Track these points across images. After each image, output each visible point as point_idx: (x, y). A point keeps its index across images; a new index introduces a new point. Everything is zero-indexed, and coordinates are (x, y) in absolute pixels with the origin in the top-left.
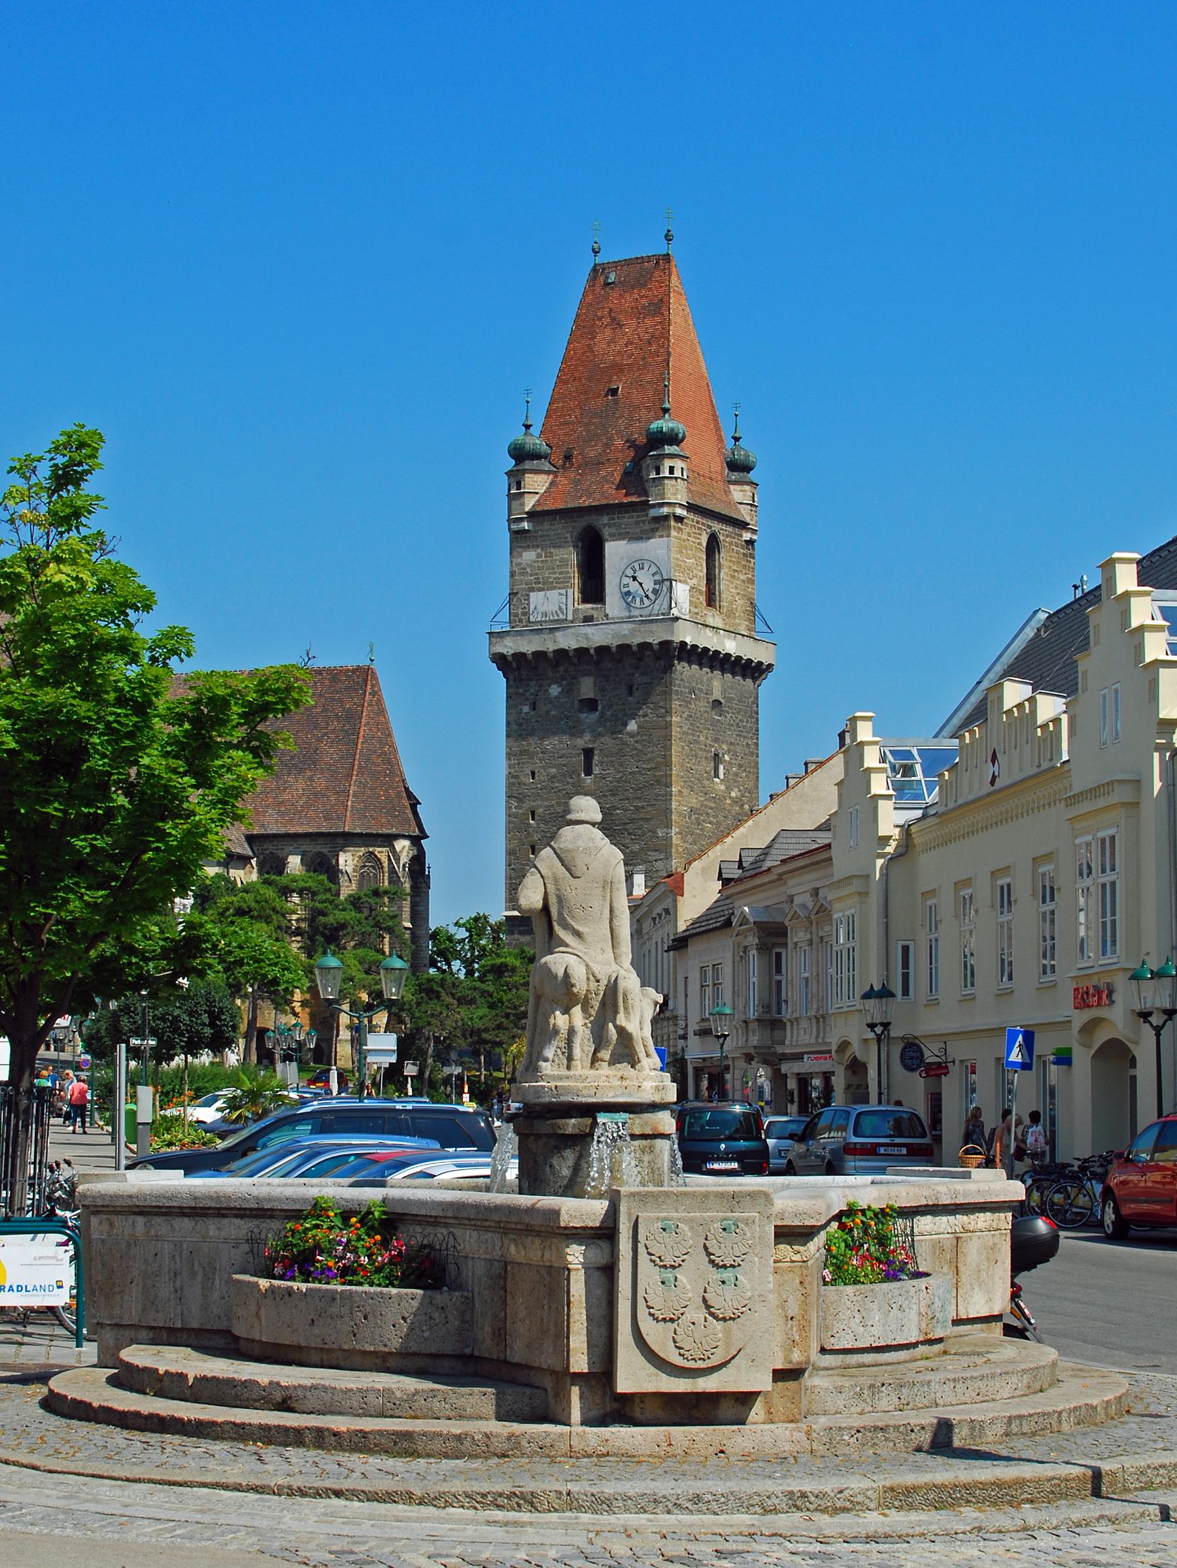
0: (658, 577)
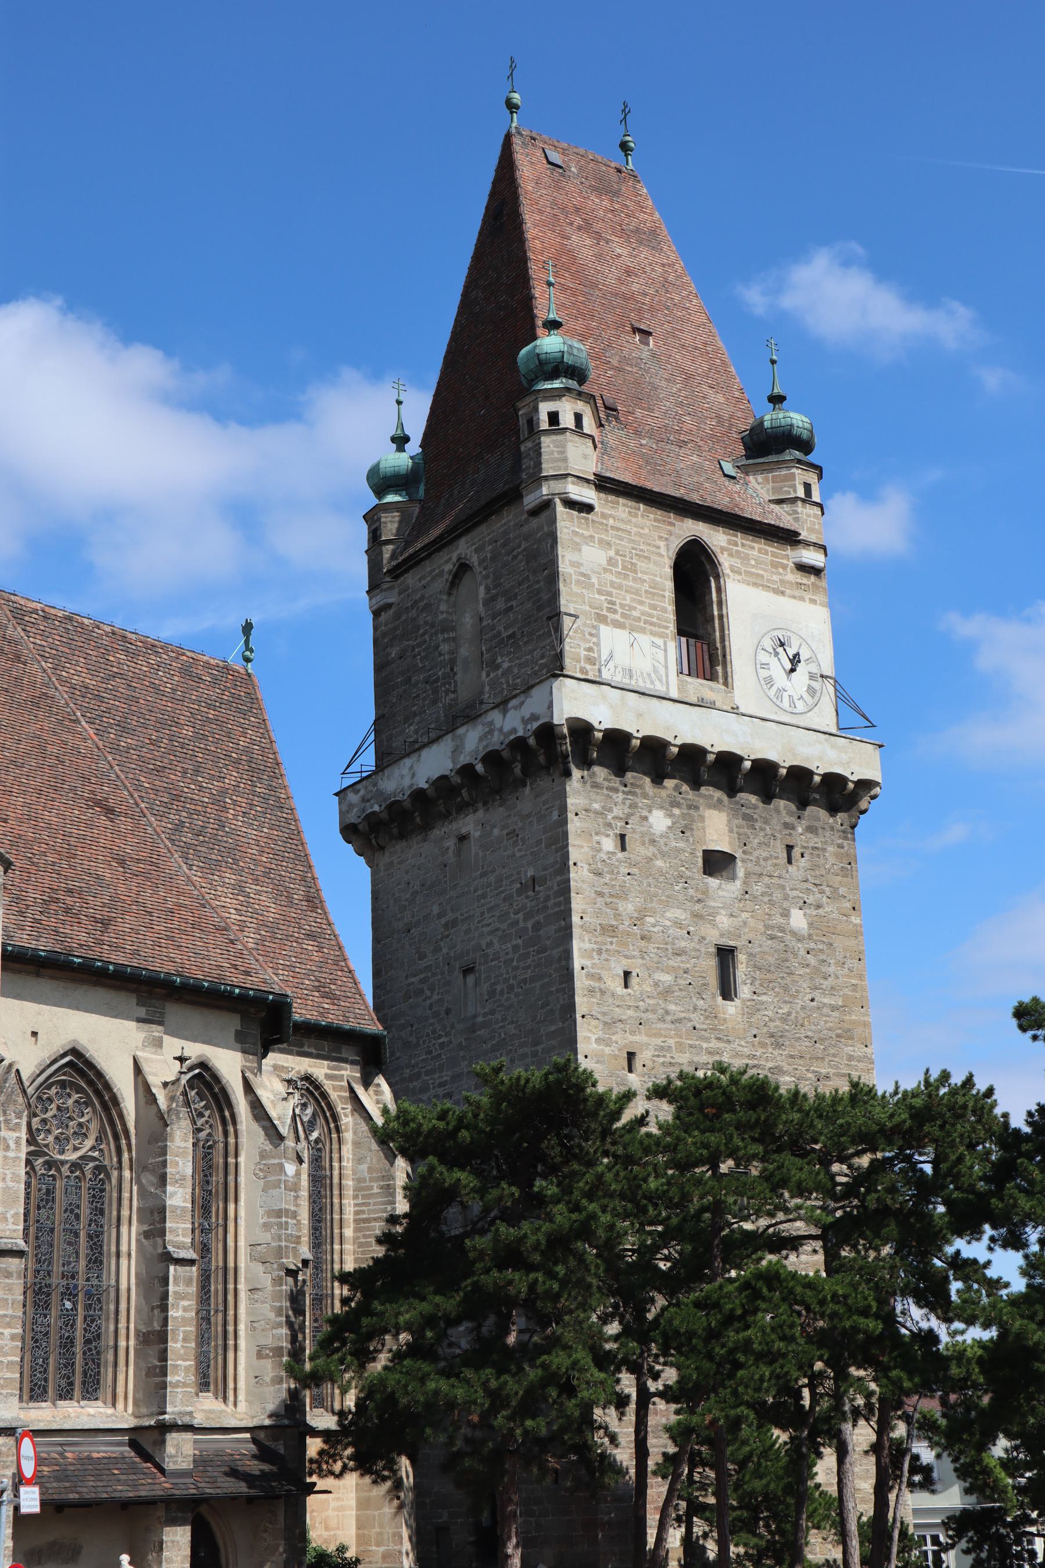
0: (814, 669)
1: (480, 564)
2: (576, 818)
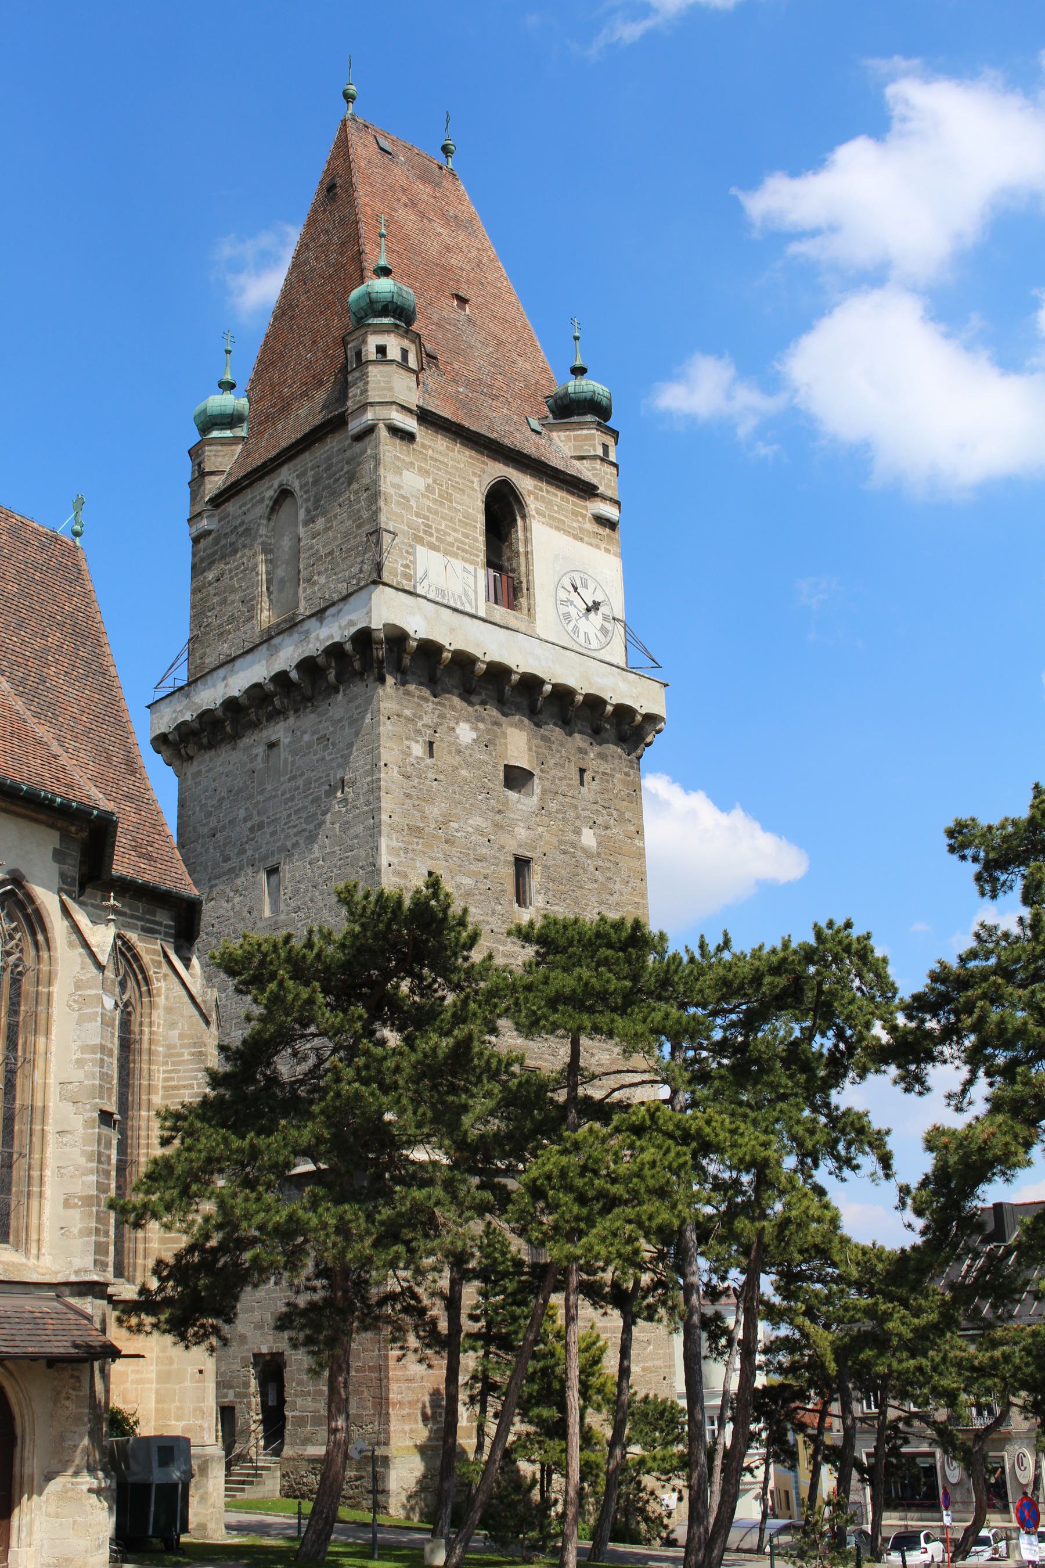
1: (301, 488)
2: (388, 722)
